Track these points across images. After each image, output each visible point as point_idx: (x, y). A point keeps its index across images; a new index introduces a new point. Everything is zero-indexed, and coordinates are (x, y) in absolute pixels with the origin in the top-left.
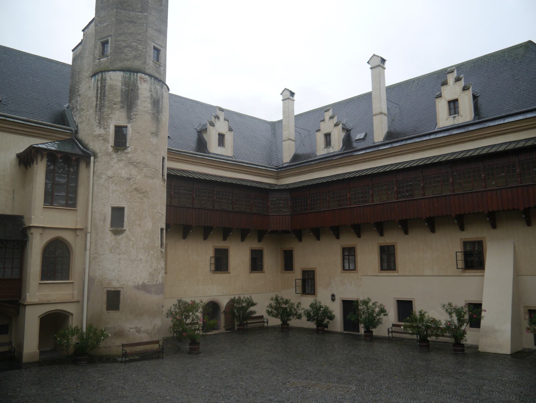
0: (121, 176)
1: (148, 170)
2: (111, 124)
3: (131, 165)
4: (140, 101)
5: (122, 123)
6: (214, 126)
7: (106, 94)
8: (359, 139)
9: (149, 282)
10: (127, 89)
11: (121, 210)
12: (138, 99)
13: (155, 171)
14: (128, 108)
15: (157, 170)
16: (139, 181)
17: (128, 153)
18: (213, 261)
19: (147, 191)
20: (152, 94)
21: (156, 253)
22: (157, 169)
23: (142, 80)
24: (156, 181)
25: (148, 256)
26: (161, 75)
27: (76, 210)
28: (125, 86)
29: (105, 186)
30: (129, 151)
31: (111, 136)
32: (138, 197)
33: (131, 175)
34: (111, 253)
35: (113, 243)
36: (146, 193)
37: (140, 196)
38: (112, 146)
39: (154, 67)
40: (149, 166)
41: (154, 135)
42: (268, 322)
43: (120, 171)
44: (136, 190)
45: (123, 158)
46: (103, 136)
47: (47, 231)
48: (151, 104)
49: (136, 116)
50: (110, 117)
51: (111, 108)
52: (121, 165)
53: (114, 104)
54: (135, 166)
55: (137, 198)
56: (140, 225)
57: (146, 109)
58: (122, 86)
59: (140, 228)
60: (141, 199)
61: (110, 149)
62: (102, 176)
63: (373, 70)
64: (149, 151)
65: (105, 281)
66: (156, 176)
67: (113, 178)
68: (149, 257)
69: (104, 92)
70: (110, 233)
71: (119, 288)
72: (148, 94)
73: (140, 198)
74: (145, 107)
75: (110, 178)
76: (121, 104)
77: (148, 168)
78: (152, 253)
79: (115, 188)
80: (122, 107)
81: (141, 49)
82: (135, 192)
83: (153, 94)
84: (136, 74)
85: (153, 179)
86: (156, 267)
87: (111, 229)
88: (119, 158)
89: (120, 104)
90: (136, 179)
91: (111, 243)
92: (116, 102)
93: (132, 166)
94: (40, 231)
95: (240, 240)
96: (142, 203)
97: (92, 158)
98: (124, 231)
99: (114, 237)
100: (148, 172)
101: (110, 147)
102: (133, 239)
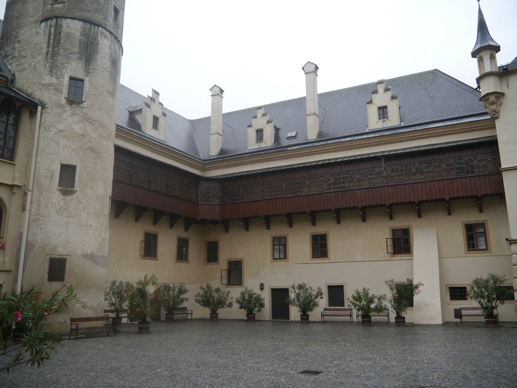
0: (74, 132)
1: (103, 130)
2: (66, 75)
3: (87, 121)
4: (99, 56)
5: (79, 74)
6: (150, 108)
7: (62, 41)
8: (291, 137)
9: (97, 252)
10: (87, 40)
11: (73, 168)
12: (97, 53)
14: (86, 61)
16: (94, 140)
17: (84, 108)
18: (143, 246)
20: (111, 52)
23: (103, 35)
27: (14, 165)
28: (85, 37)
29: (55, 140)
30: (85, 105)
31: (64, 87)
32: (92, 157)
33: (85, 132)
34: (59, 215)
35: (61, 204)
37: (94, 156)
38: (65, 98)
41: (111, 95)
42: (192, 314)
43: (73, 126)
44: (90, 148)
45: (78, 113)
46: (55, 86)
48: (110, 62)
49: (94, 71)
50: (64, 67)
51: (67, 57)
52: (75, 119)
53: (71, 54)
54: (91, 123)
55: (90, 158)
56: (92, 187)
58: (81, 36)
61: (64, 101)
62: (51, 129)
63: (308, 75)
65: (48, 247)
67: (65, 132)
69: (59, 40)
70: (58, 193)
71: (65, 255)
72: (108, 51)
73: (94, 158)
74: (104, 63)
75: (61, 132)
76: (79, 55)
77: (103, 128)
78: (102, 221)
79: (67, 143)
80: (80, 58)
81: (102, 4)
82: (89, 151)
84: (97, 27)
85: (107, 141)
87: (59, 188)
88: (73, 112)
89: (78, 55)
90: (91, 137)
91: (59, 204)
92: (73, 52)
93: (87, 122)
95: (168, 226)
97: (39, 108)
98: (75, 191)
99: (62, 197)
100: (103, 131)
101: (63, 99)
102: (84, 202)
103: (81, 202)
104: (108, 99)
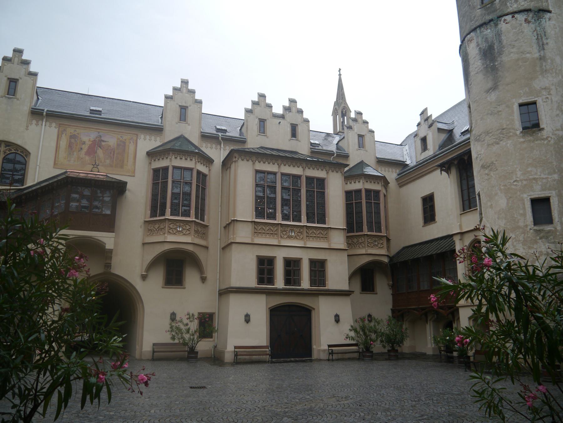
1: (490, 137)
4: (471, 66)
13: (501, 132)
15: (503, 129)
19: (492, 163)
21: (523, 235)
22: (505, 127)
24: (504, 143)
26: (497, 10)
36: (491, 165)
37: (487, 172)
39: (484, 12)
40: (490, 131)
41: (491, 91)
48: (480, 60)
56: (491, 206)
57: (476, 69)
60: (488, 175)
64: (488, 114)
66: (504, 137)
73: (487, 174)
77: (489, 135)
82: (482, 170)
83: (481, 46)
85: (498, 144)
90: (481, 154)
96: (489, 179)
100: (490, 139)
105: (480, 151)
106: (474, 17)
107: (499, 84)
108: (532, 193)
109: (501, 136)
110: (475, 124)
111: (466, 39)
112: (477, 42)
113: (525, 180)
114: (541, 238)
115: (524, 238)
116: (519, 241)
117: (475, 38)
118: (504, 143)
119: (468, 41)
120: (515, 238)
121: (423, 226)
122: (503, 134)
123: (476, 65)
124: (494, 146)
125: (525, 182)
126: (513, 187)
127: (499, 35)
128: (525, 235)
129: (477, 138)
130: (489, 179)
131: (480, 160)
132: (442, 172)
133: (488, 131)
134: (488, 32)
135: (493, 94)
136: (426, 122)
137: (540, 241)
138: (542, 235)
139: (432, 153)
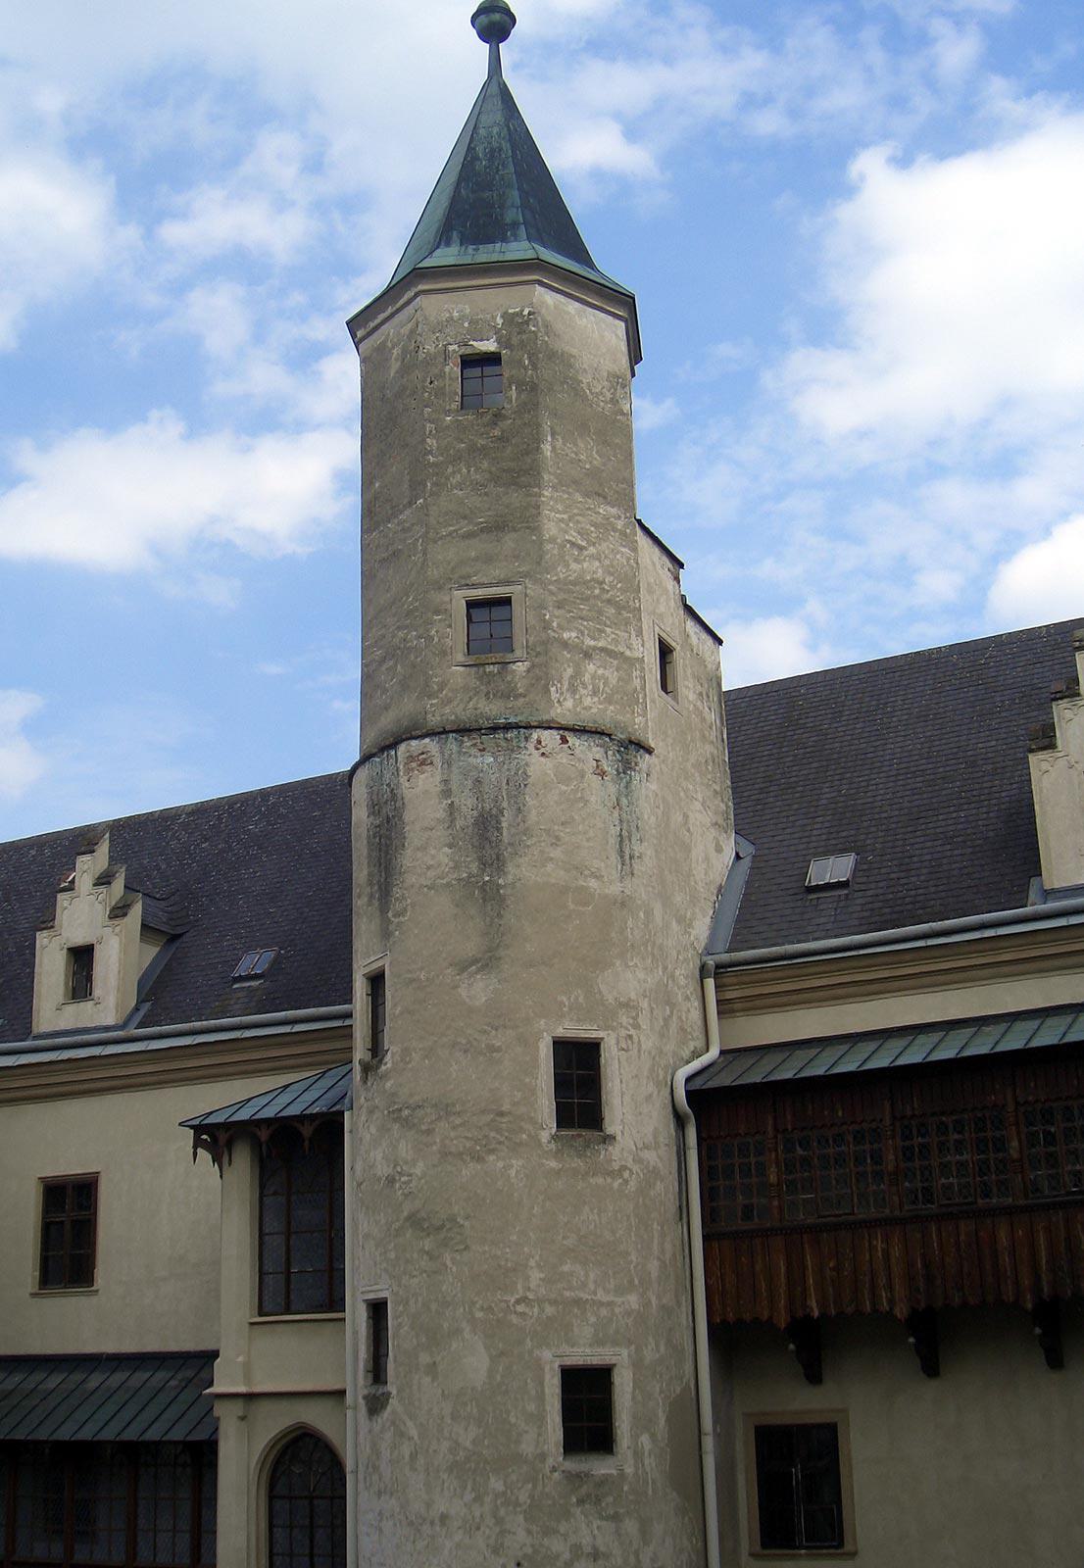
1: (454, 1128)
3: (395, 1120)
4: (409, 852)
13: (493, 1120)
15: (501, 1114)
17: (385, 1077)
19: (452, 1219)
21: (530, 1486)
22: (506, 1107)
24: (500, 1164)
25: (475, 1500)
26: (516, 697)
32: (422, 1251)
37: (427, 1244)
39: (474, 682)
40: (458, 1108)
44: (415, 1221)
47: (265, 1406)
49: (402, 919)
54: (407, 1124)
55: (415, 1255)
56: (432, 1369)
57: (431, 874)
59: (433, 1381)
66: (500, 1143)
68: (482, 1505)
72: (435, 810)
73: (427, 1253)
74: (428, 868)
78: (501, 1488)
85: (480, 1159)
86: (530, 1551)
90: (410, 1175)
93: (396, 1126)
94: (237, 1408)
96: (435, 1272)
100: (452, 1134)
102: (414, 1433)
103: (402, 1434)
104: (464, 994)
105: (406, 1163)
106: (442, 686)
107: (502, 952)
108: (568, 1350)
109: (493, 1134)
110: (397, 1058)
111: (402, 747)
112: (446, 782)
113: (554, 1303)
114: (581, 1502)
115: (531, 1496)
116: (517, 1504)
117: (438, 761)
118: (500, 1164)
119: (411, 758)
120: (504, 1493)
121: (34, 1295)
122: (499, 1131)
123: (433, 857)
124: (464, 1162)
125: (550, 1310)
126: (514, 1319)
127: (518, 784)
128: (535, 1486)
129: (400, 1110)
130: (435, 1272)
131: (406, 1196)
132: (199, 1150)
133: (447, 1105)
134: (484, 760)
135: (481, 984)
136: (102, 889)
137: (578, 1511)
138: (584, 1490)
139: (110, 1019)
